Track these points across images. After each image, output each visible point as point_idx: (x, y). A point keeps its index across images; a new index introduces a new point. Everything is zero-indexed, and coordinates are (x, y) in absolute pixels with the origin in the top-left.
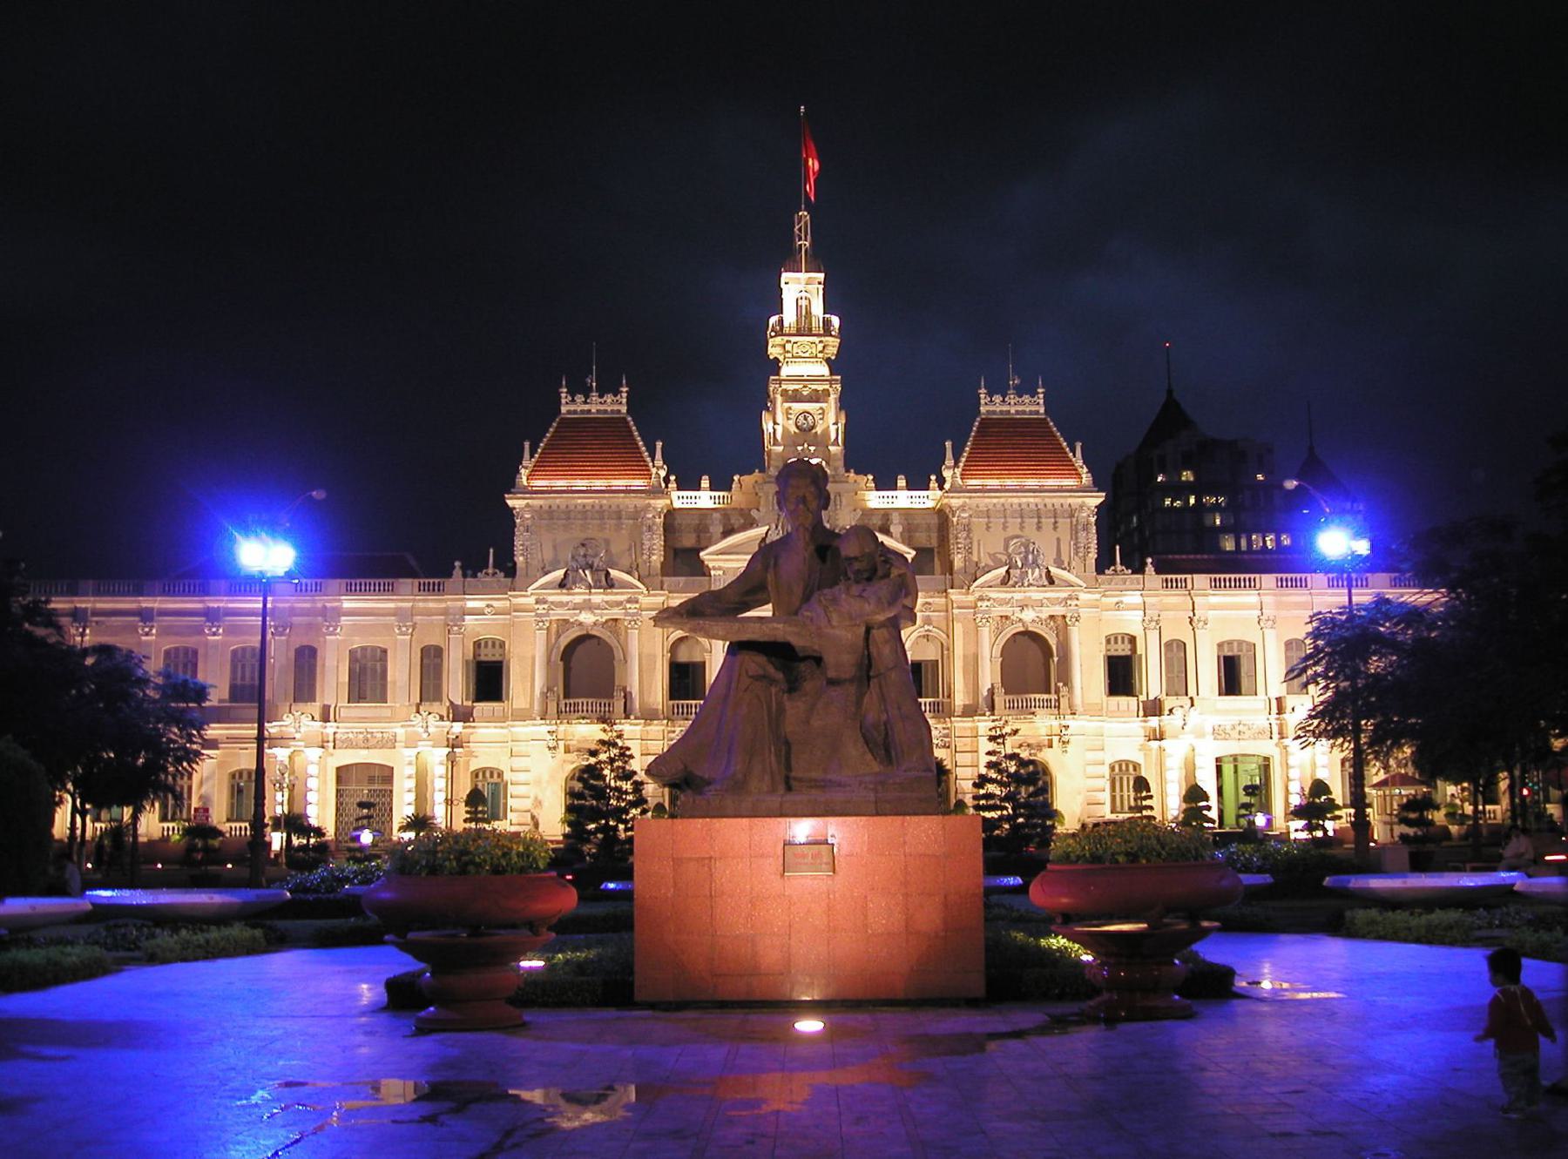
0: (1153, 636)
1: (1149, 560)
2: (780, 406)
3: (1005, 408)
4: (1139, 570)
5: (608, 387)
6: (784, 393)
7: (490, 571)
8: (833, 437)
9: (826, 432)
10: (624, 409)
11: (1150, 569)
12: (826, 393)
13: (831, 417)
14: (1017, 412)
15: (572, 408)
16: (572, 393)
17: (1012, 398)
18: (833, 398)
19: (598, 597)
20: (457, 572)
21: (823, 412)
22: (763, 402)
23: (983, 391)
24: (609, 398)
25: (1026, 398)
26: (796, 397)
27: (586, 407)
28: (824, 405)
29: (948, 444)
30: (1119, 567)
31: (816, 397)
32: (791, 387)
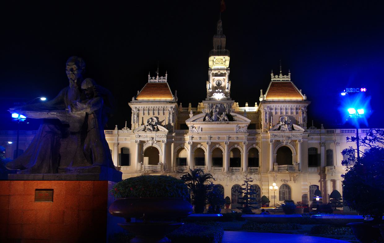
0: (323, 148)
1: (322, 125)
2: (211, 78)
3: (279, 79)
4: (319, 127)
5: (162, 74)
6: (213, 73)
7: (125, 128)
8: (227, 88)
9: (225, 87)
10: (166, 81)
11: (322, 127)
12: (225, 74)
13: (227, 80)
14: (282, 80)
15: (151, 80)
16: (151, 76)
17: (281, 75)
18: (227, 75)
19: (154, 134)
20: (116, 128)
21: (224, 80)
22: (207, 79)
23: (272, 74)
24: (162, 77)
25: (285, 76)
26: (216, 75)
27: (155, 80)
28: (224, 77)
29: (261, 91)
30: (313, 127)
31: (222, 75)
32: (215, 72)
